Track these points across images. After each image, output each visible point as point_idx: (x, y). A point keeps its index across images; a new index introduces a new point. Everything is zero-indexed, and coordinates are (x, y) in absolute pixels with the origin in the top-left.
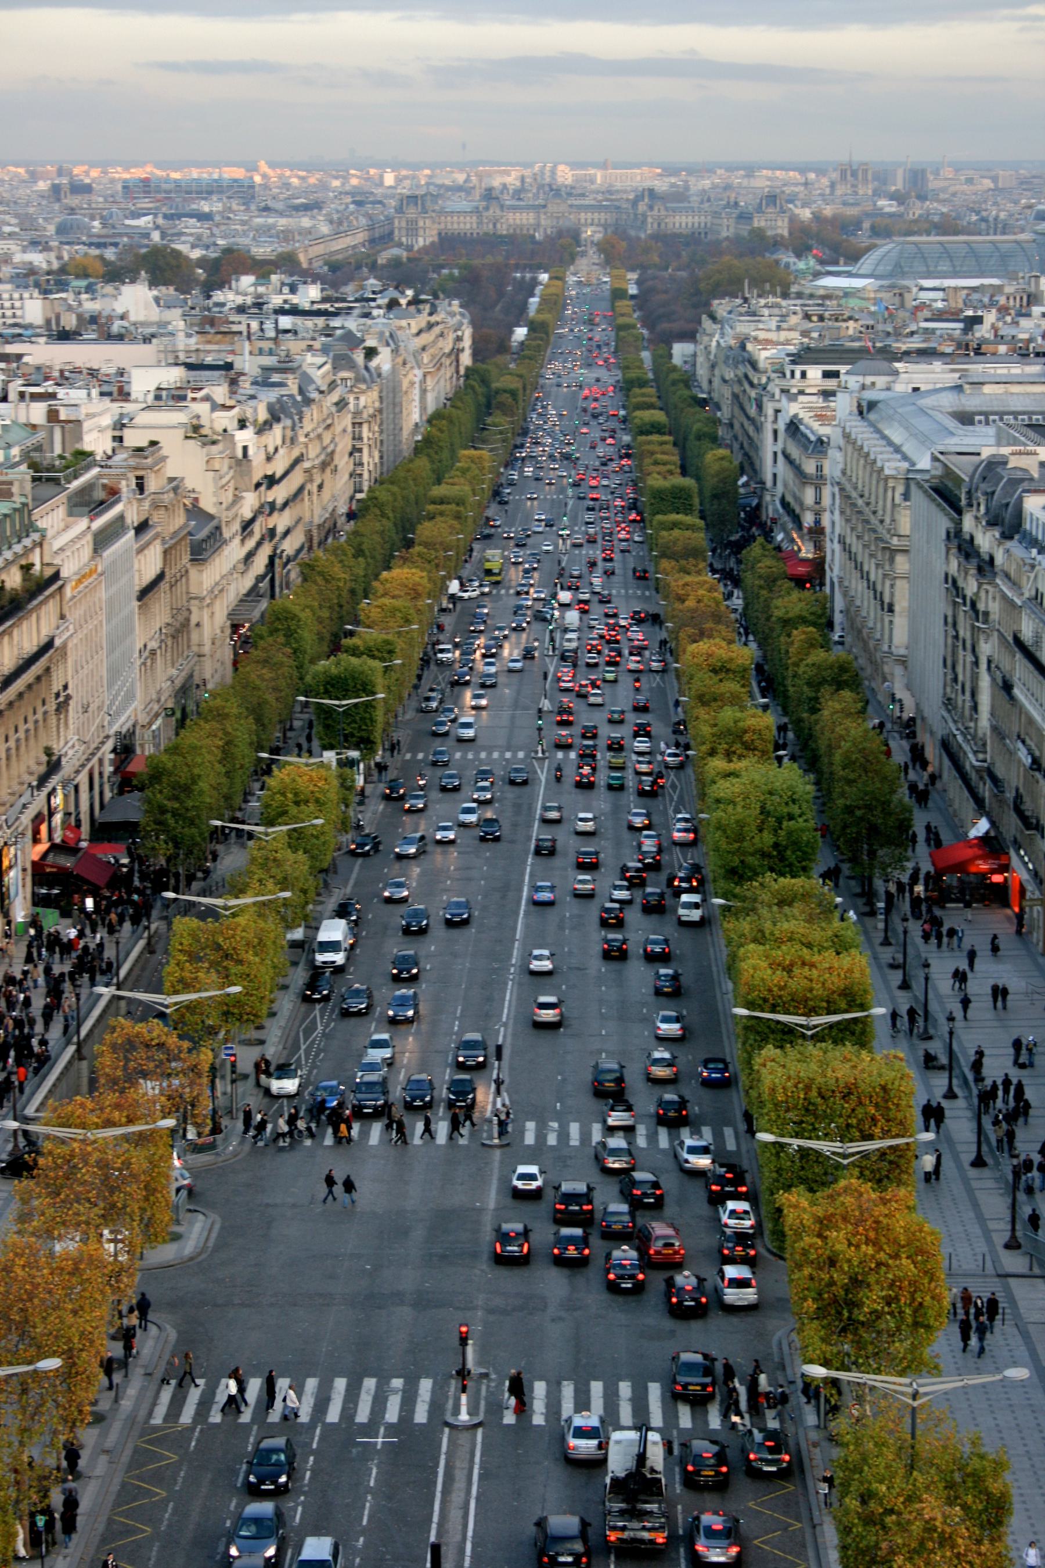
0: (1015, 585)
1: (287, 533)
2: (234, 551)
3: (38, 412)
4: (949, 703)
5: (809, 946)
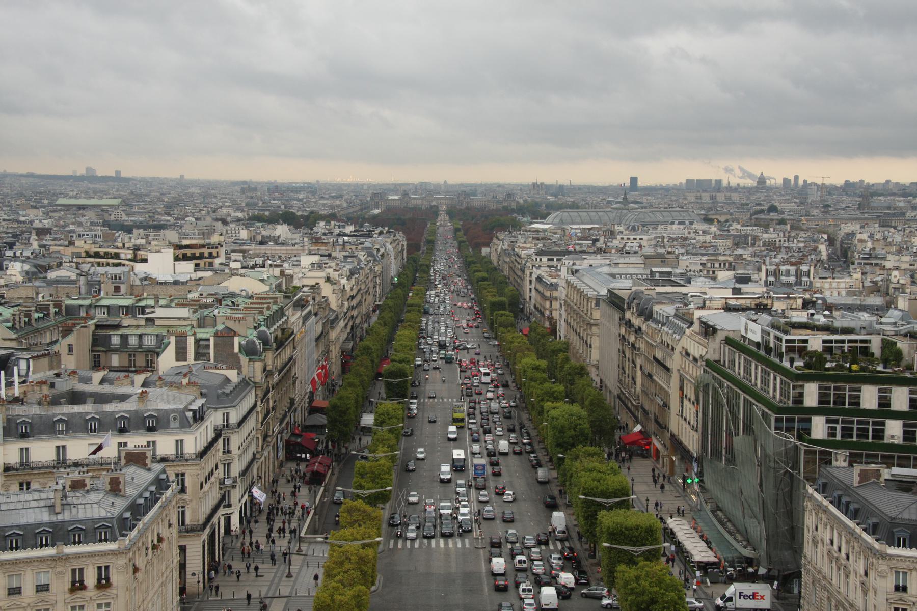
0: (653, 338)
1: (356, 317)
2: (342, 324)
3: (277, 272)
4: (620, 381)
5: (604, 473)
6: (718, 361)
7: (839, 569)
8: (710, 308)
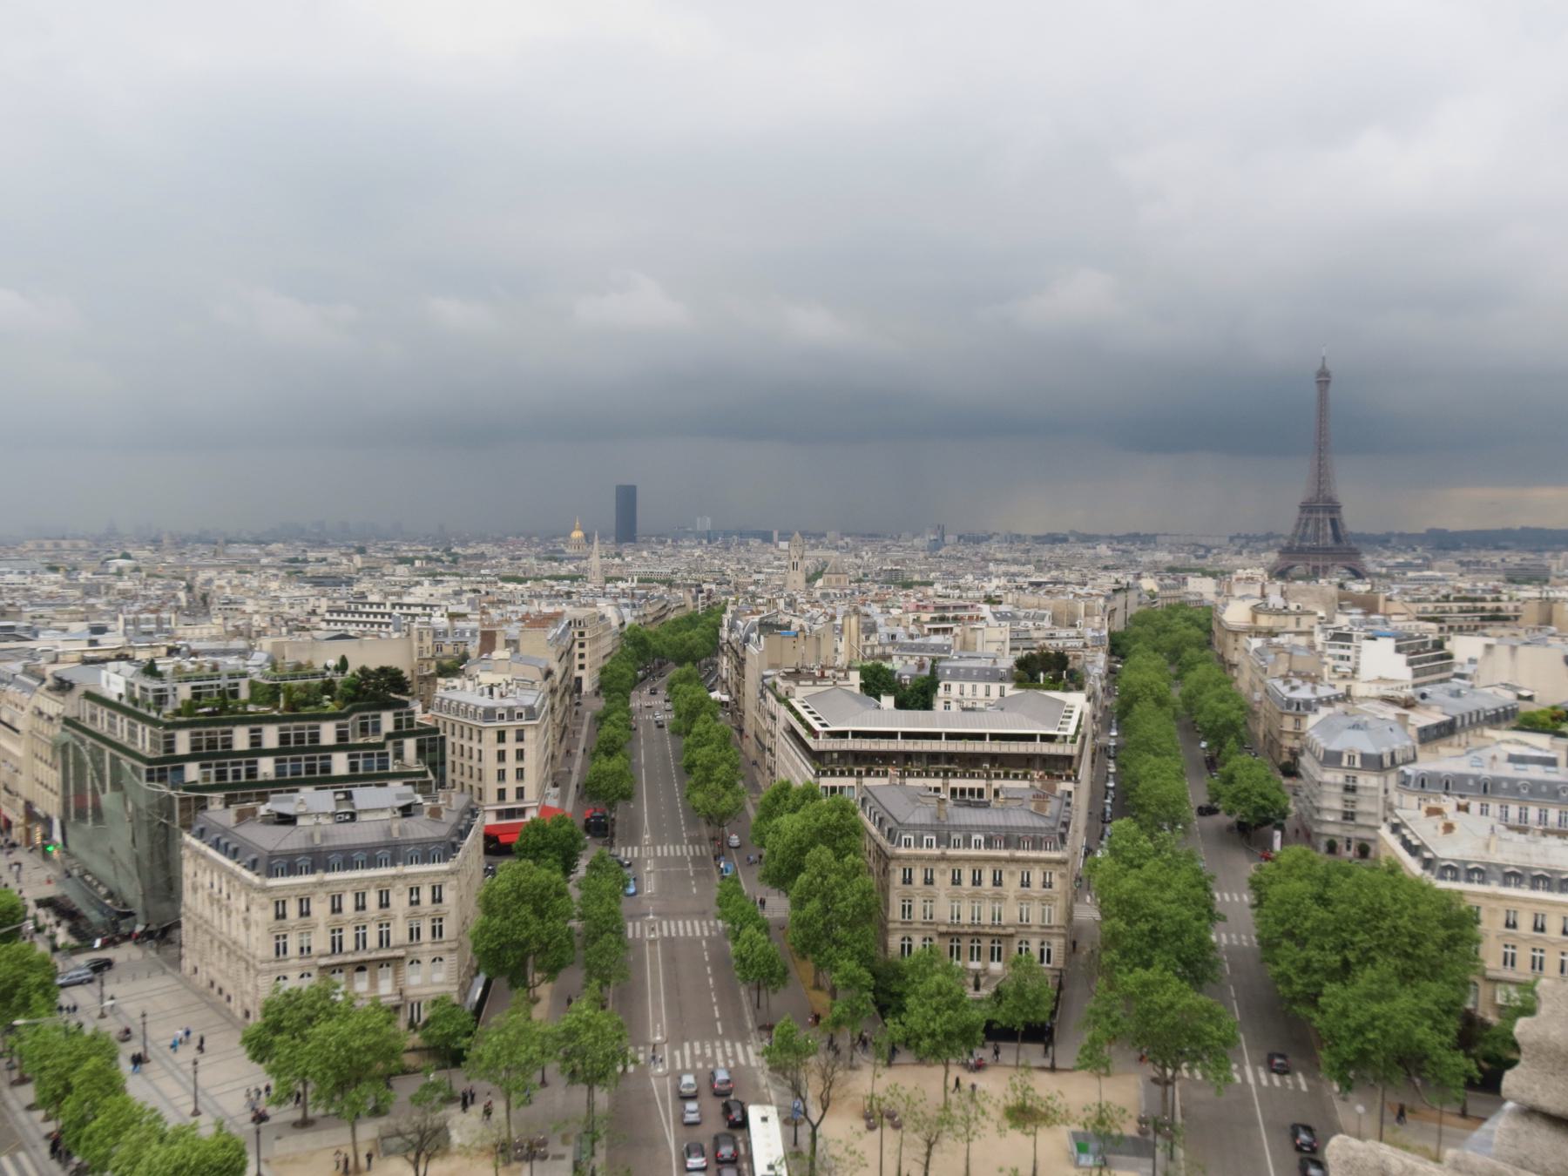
6: (78, 718)
7: (220, 910)
8: (65, 662)
